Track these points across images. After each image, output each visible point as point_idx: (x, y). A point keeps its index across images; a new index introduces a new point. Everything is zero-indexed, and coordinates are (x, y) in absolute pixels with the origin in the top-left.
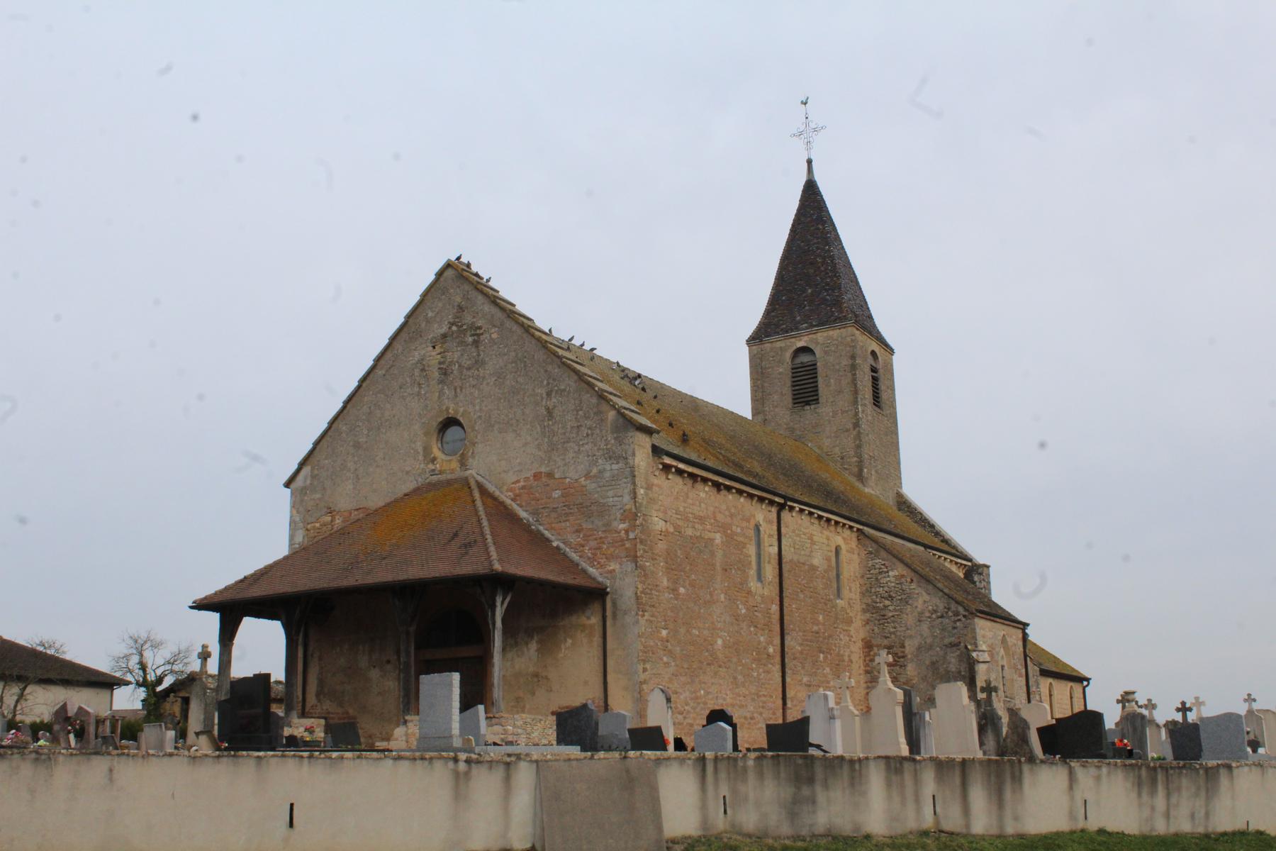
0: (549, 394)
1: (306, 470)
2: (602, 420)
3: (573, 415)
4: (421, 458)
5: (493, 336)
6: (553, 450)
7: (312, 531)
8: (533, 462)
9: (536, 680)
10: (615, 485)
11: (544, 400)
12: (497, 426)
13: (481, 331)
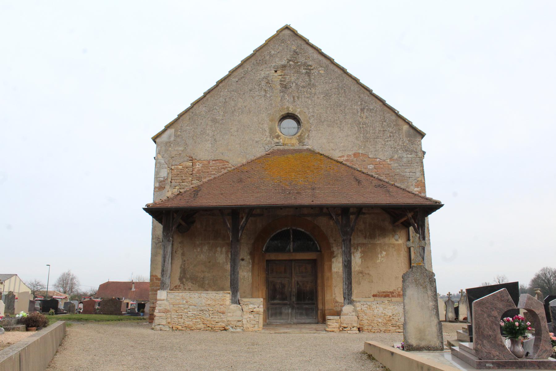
0: (362, 110)
1: (171, 131)
2: (399, 130)
3: (380, 124)
4: (267, 134)
5: (320, 72)
6: (367, 141)
7: (175, 171)
8: (353, 147)
9: (361, 275)
10: (410, 166)
11: (359, 114)
12: (325, 123)
13: (312, 68)
